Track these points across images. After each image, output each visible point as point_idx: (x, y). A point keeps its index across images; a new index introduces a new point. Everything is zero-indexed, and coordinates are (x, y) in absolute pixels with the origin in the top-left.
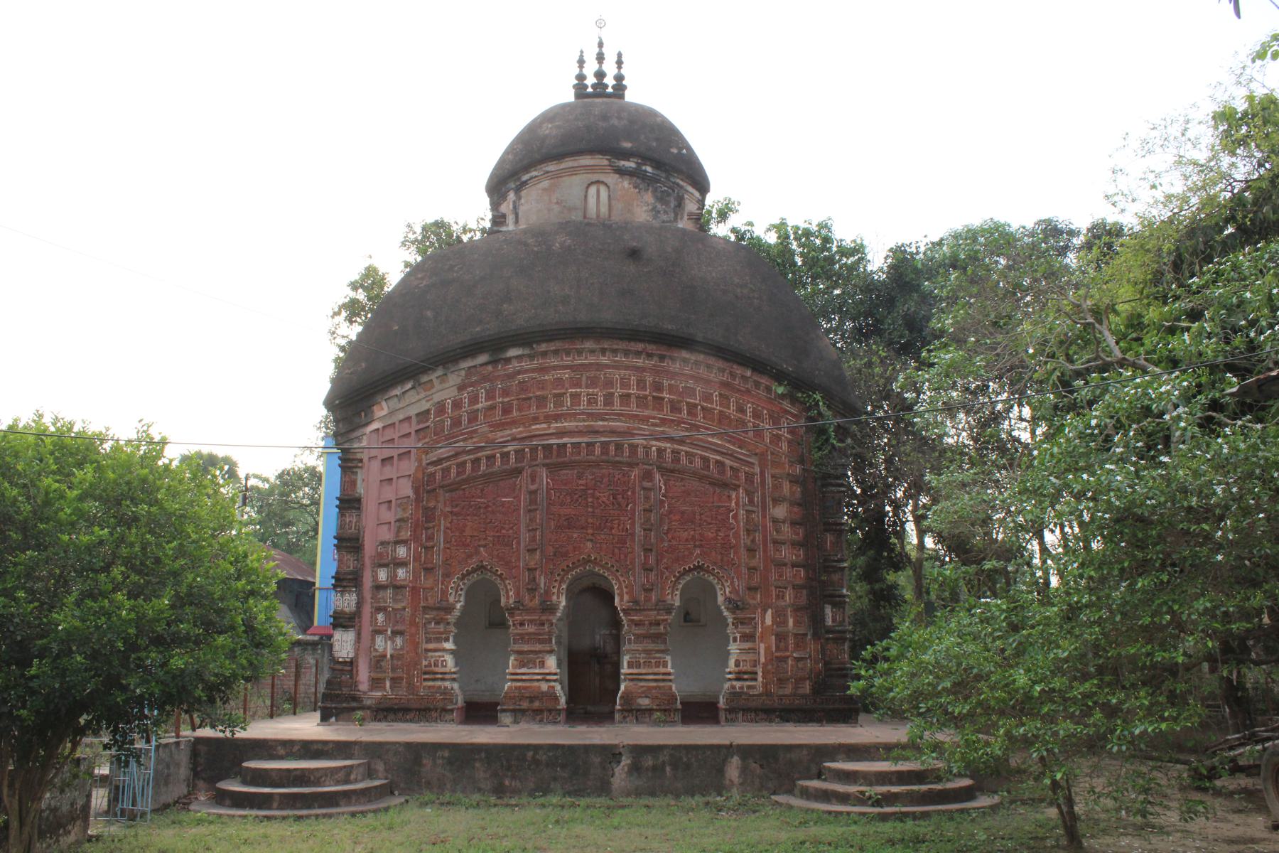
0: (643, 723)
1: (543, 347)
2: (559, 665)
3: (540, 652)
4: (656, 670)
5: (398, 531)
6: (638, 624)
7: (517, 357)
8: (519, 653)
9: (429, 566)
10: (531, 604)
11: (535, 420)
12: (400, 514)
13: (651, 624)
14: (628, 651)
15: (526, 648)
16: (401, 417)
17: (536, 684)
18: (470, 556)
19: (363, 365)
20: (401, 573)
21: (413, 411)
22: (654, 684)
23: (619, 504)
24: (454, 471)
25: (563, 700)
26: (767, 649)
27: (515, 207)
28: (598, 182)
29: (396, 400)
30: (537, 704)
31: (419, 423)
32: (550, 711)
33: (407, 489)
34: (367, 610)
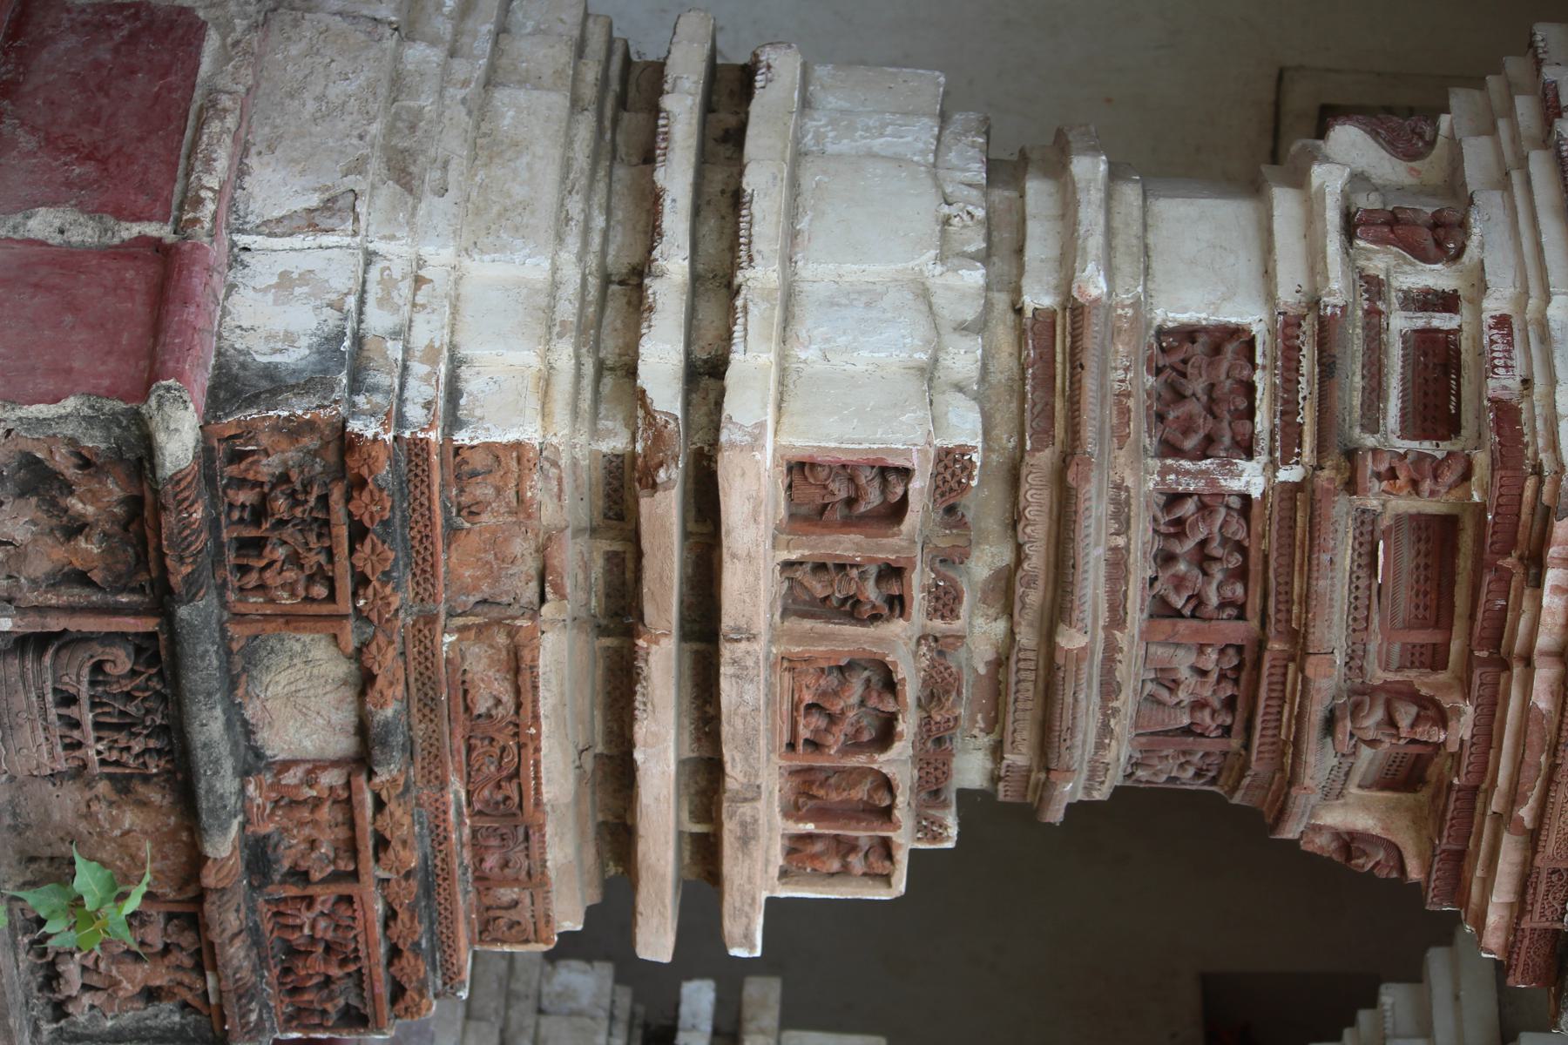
22: (558, 774)
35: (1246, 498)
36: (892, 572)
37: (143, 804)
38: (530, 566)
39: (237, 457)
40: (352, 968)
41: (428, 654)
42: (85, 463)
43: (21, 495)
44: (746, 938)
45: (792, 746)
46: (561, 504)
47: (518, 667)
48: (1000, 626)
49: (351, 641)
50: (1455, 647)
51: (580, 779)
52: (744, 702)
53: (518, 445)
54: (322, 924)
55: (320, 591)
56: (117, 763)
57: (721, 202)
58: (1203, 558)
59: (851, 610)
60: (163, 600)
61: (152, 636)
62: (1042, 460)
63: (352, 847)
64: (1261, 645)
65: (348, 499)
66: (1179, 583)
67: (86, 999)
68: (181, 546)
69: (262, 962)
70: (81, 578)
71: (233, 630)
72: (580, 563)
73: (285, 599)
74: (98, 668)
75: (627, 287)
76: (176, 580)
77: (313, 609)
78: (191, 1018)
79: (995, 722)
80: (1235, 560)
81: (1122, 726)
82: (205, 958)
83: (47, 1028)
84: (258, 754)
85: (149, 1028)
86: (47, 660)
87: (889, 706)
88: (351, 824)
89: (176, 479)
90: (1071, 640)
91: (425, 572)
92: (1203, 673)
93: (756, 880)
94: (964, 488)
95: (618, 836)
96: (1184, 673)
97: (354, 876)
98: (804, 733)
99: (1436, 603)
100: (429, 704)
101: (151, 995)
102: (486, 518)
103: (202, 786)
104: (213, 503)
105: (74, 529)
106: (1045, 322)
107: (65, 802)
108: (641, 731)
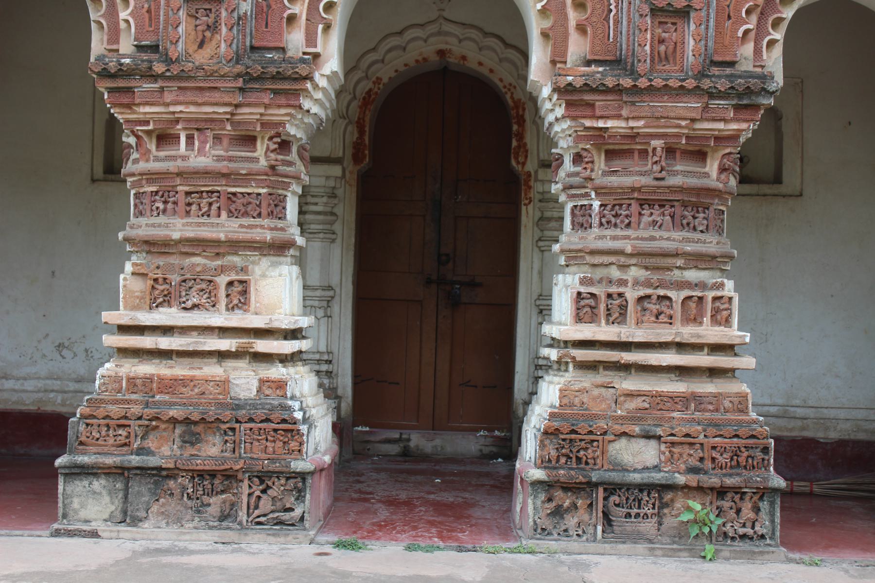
0: (636, 538)
2: (316, 297)
3: (235, 246)
4: (687, 333)
6: (617, 151)
8: (152, 246)
10: (202, 57)
13: (670, 151)
14: (575, 256)
15: (178, 228)
17: (212, 370)
25: (319, 442)
30: (212, 450)
32: (263, 477)
35: (601, 205)
36: (609, 296)
37: (672, 500)
38: (603, 390)
39: (550, 461)
40: (743, 449)
41: (622, 417)
42: (550, 500)
43: (563, 518)
45: (671, 324)
46: (587, 380)
47: (631, 395)
48: (633, 268)
49: (612, 437)
50: (639, 147)
51: (681, 380)
52: (643, 336)
53: (560, 390)
54: (725, 456)
55: (595, 444)
56: (654, 505)
58: (616, 216)
59: (623, 307)
60: (592, 485)
61: (605, 490)
62: (589, 259)
63: (691, 444)
64: (638, 199)
65: (562, 433)
66: (622, 222)
67: (756, 528)
68: (572, 477)
69: (738, 474)
70: (590, 505)
71: (605, 468)
72: (602, 377)
73: (598, 453)
74: (618, 505)
76: (584, 480)
77: (601, 446)
78: (765, 498)
79: (669, 269)
80: (617, 207)
81: (666, 235)
82: (737, 490)
83: (768, 541)
84: (656, 466)
85: (770, 512)
86: (613, 519)
87: (655, 297)
88: (682, 443)
89: (549, 476)
90: (629, 250)
91: (595, 417)
92: (652, 214)
94: (591, 279)
96: (651, 219)
97: (702, 444)
98: (666, 320)
99: (625, 153)
100: (641, 419)
101: (757, 510)
102: (585, 400)
103: (657, 482)
104: (562, 468)
105: (574, 506)
106: (568, 259)
107: (669, 522)
108: (655, 363)
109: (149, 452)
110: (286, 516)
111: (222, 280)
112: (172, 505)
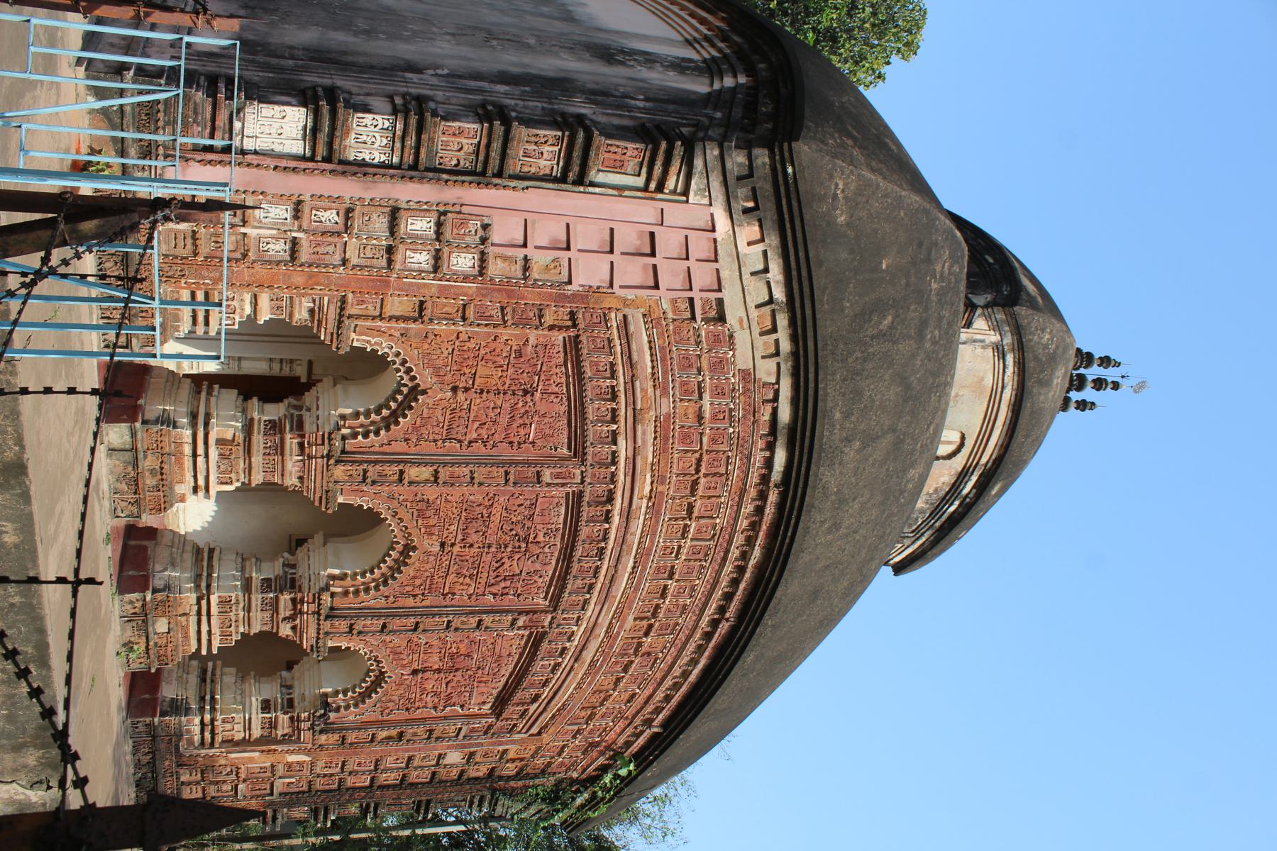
0: (123, 630)
1: (773, 497)
5: (505, 258)
7: (769, 464)
9: (427, 313)
11: (658, 479)
12: (540, 259)
16: (724, 274)
18: (436, 372)
19: (842, 219)
20: (422, 259)
21: (731, 296)
23: (497, 583)
24: (604, 360)
26: (252, 760)
27: (975, 341)
28: (962, 445)
29: (761, 267)
30: (150, 481)
31: (707, 301)
33: (589, 273)
34: (349, 188)
44: (215, 651)
57: (210, 566)
75: (199, 576)
82: (149, 657)
93: (216, 644)
95: (199, 640)
109: (145, 457)
110: (119, 510)
111: (233, 475)
112: (120, 469)
